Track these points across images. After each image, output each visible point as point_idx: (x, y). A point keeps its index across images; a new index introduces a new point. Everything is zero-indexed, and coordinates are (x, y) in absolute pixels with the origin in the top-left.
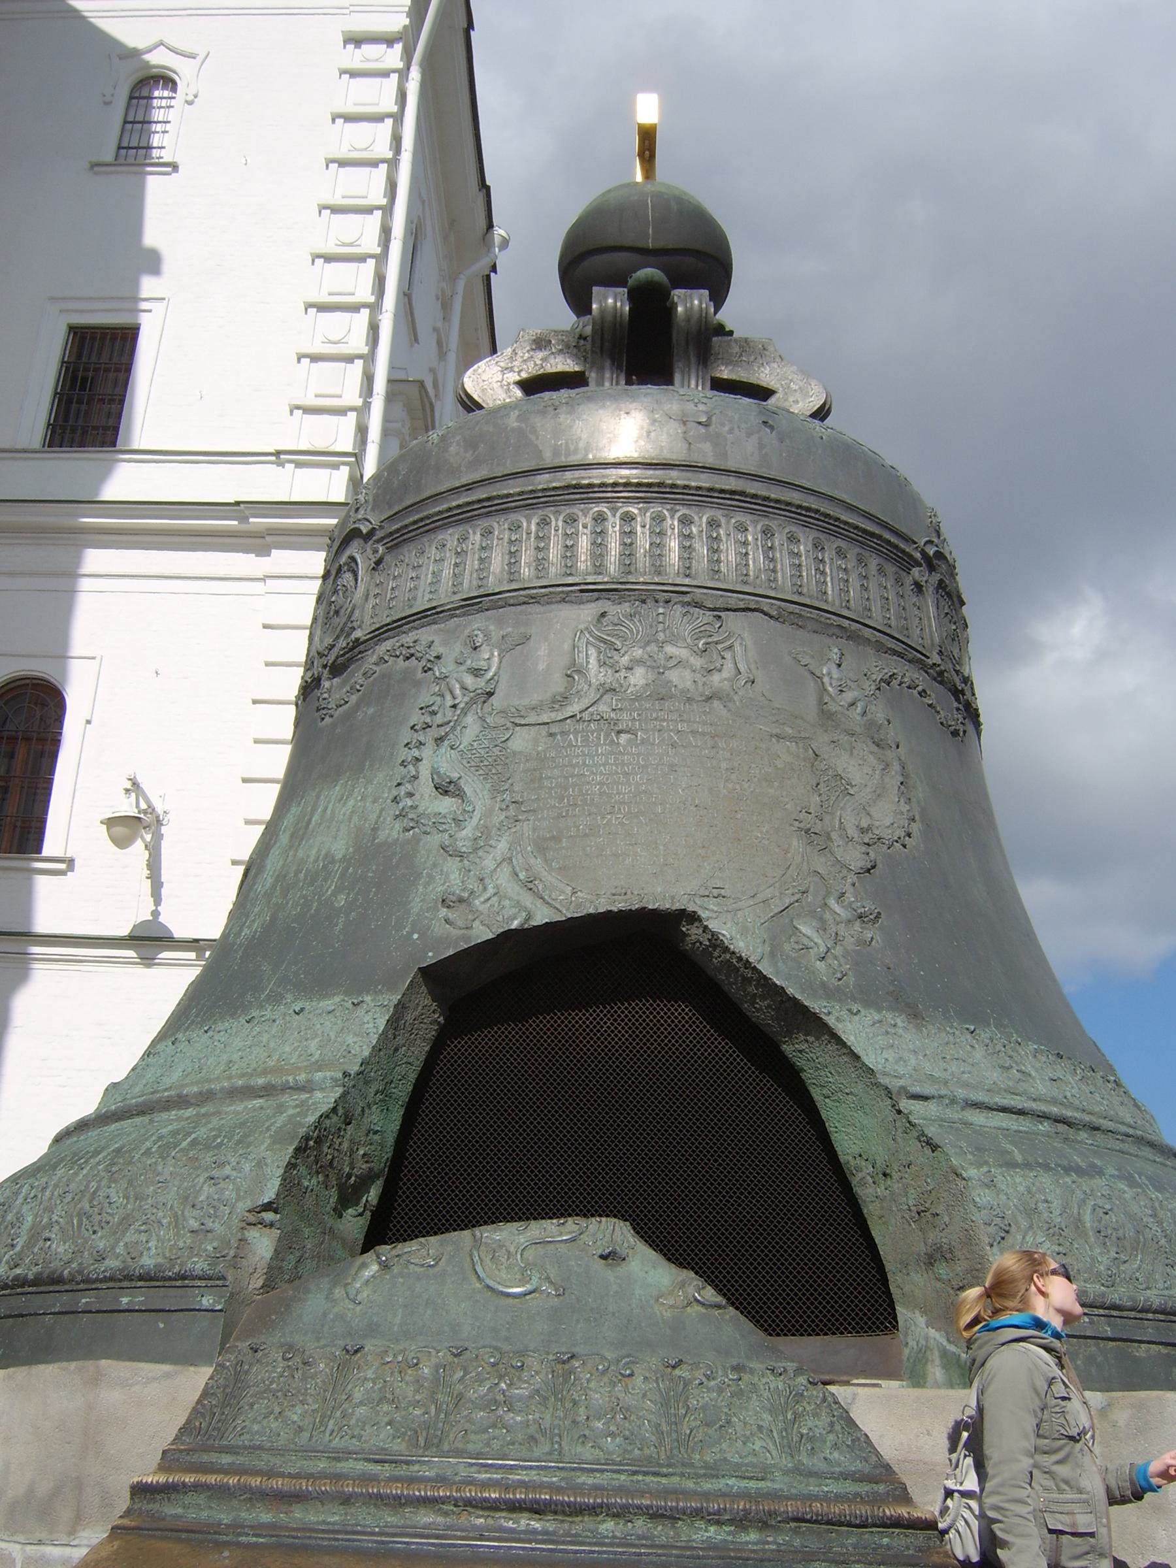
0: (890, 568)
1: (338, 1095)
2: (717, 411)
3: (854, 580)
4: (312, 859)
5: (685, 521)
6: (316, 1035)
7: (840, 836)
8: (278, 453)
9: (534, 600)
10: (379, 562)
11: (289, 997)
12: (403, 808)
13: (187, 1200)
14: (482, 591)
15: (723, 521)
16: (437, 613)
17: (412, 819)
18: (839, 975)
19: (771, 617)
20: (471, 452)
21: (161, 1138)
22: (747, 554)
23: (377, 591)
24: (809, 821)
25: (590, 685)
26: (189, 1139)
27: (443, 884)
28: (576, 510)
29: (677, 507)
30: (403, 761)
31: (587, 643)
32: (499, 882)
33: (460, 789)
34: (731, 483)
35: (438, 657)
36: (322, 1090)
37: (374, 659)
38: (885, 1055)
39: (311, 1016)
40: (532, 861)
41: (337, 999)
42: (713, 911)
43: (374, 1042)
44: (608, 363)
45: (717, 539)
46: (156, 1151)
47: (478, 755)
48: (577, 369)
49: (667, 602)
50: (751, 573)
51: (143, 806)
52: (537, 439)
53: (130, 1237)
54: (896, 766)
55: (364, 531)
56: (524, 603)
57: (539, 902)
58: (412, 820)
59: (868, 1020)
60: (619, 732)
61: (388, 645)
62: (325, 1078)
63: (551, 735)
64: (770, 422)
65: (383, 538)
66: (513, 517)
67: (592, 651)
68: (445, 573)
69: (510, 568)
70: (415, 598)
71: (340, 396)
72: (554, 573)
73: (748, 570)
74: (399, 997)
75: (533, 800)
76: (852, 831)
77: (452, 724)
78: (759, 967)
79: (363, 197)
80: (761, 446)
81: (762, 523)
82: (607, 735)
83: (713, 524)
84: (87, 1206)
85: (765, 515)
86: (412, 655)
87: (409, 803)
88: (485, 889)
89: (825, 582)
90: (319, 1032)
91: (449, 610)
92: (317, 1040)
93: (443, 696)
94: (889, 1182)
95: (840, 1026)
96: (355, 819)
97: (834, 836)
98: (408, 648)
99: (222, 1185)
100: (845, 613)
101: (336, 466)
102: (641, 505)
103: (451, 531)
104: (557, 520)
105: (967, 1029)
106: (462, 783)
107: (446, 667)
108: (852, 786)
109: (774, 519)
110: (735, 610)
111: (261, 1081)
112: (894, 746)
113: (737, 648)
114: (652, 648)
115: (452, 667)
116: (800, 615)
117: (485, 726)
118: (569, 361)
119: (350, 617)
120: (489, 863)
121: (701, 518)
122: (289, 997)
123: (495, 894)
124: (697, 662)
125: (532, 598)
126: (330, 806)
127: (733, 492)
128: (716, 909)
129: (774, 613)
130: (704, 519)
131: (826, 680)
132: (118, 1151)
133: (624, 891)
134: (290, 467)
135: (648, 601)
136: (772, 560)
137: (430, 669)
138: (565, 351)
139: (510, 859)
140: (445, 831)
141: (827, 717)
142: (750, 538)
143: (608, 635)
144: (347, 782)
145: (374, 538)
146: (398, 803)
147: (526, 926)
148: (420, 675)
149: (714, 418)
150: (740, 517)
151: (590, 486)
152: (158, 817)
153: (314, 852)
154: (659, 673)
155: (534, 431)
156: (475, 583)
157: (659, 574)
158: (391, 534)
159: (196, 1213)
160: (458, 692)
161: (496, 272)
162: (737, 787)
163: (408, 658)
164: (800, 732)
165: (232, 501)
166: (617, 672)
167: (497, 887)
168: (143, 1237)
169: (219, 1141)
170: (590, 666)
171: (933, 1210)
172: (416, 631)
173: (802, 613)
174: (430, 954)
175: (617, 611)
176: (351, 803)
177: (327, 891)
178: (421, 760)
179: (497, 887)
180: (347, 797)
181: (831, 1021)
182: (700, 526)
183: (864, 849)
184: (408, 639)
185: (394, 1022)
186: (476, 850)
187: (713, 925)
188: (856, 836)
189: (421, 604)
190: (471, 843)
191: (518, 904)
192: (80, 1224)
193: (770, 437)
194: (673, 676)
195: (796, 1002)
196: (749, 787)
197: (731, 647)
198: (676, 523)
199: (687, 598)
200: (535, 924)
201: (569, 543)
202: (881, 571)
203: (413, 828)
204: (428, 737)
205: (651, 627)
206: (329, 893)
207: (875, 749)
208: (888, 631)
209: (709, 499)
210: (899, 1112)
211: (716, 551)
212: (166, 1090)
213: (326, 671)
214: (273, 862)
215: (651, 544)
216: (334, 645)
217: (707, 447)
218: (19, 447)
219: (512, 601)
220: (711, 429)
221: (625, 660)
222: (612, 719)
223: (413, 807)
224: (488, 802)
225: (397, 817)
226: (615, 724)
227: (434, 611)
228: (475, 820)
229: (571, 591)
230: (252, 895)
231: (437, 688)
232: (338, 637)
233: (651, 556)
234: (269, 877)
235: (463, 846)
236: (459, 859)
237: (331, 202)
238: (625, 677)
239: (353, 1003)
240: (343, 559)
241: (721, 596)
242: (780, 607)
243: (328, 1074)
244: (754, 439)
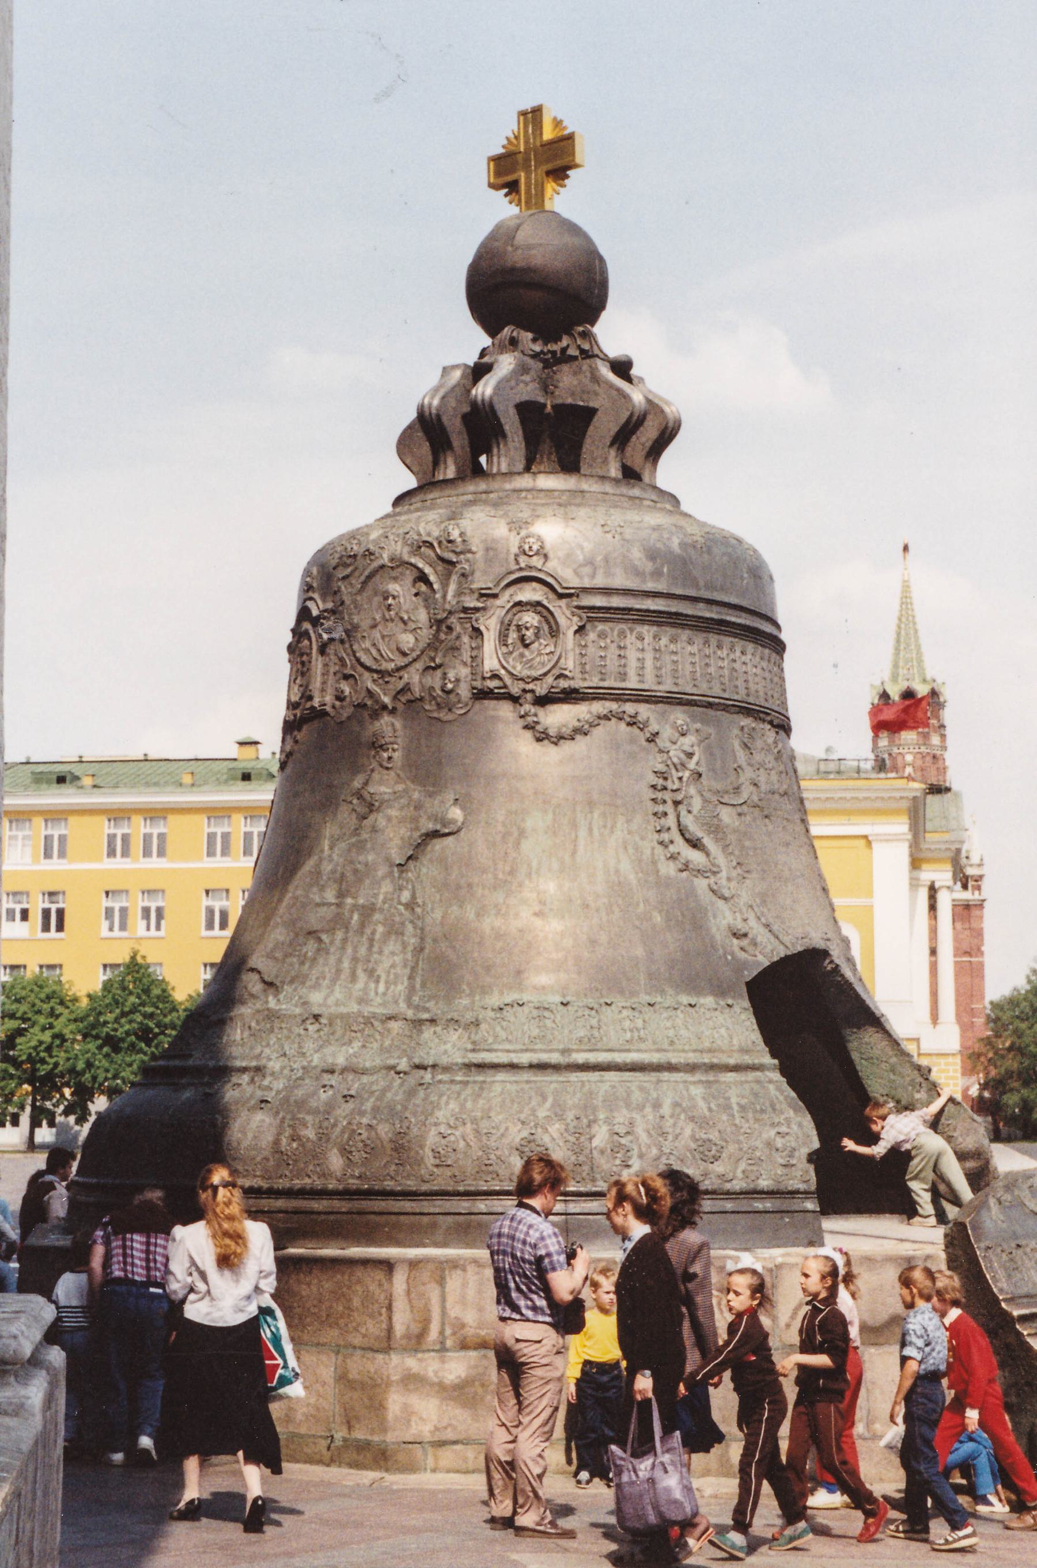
9: (710, 705)
13: (769, 1144)
33: (704, 845)
35: (657, 733)
53: (742, 1166)
56: (706, 707)
66: (688, 632)
68: (649, 664)
72: (717, 691)
84: (693, 1146)
86: (634, 723)
96: (631, 851)
99: (787, 1137)
103: (646, 627)
107: (662, 742)
115: (668, 744)
117: (706, 801)
132: (676, 1105)
137: (653, 741)
146: (666, 847)
160: (679, 767)
168: (755, 1168)
176: (618, 833)
184: (630, 708)
187: (837, 961)
189: (632, 683)
192: (694, 1157)
199: (769, 718)
204: (667, 796)
206: (642, 905)
223: (679, 853)
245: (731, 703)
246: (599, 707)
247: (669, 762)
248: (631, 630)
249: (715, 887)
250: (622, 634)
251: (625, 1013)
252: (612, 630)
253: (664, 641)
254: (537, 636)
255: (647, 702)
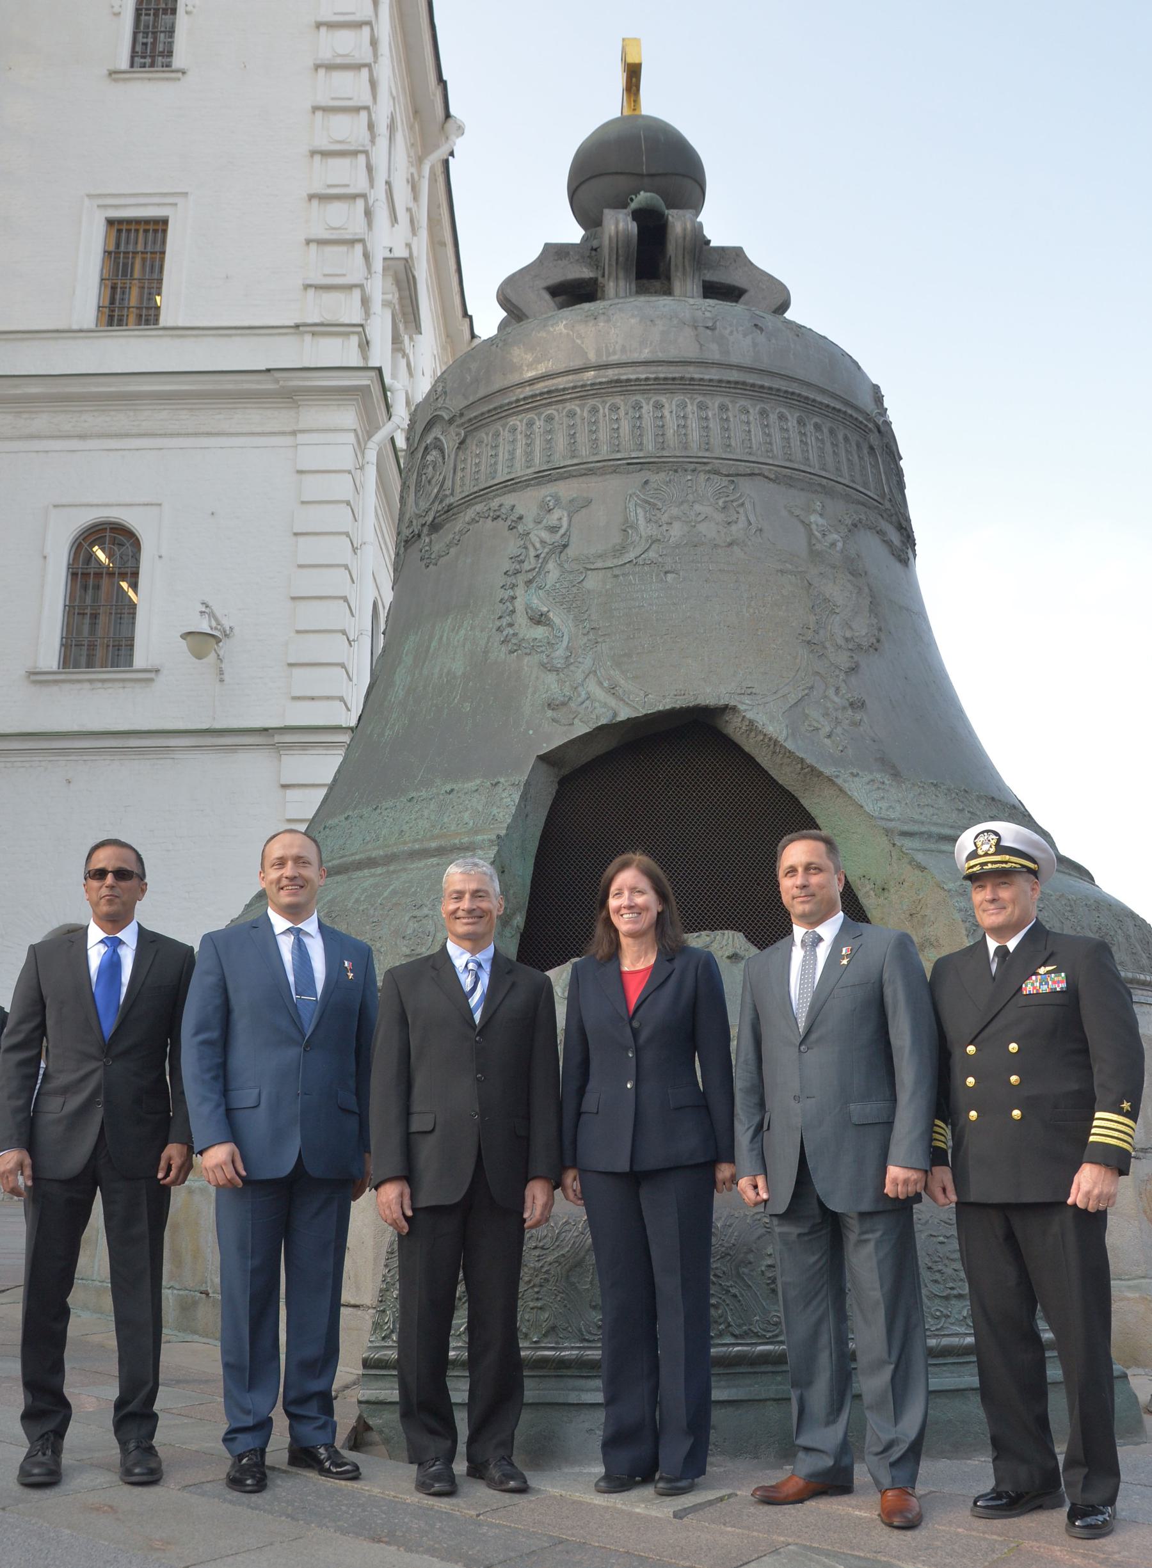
0: (854, 438)
1: (495, 852)
2: (719, 318)
3: (828, 448)
4: (436, 676)
5: (702, 407)
6: (467, 809)
7: (832, 645)
8: (297, 326)
10: (461, 443)
11: (438, 781)
12: (507, 636)
14: (550, 466)
15: (730, 406)
16: (516, 483)
17: (515, 644)
18: (840, 748)
19: (770, 479)
20: (530, 354)
21: (365, 890)
22: (749, 431)
23: (463, 466)
24: (809, 635)
25: (641, 537)
26: (389, 890)
27: (547, 691)
28: (618, 400)
29: (695, 396)
30: (502, 599)
31: (636, 504)
32: (589, 689)
33: (549, 619)
34: (734, 376)
35: (521, 518)
36: (481, 848)
37: (467, 519)
38: (879, 805)
39: (460, 795)
40: (612, 672)
41: (478, 782)
42: (748, 705)
43: (514, 812)
44: (621, 275)
45: (727, 420)
46: (364, 901)
47: (560, 593)
48: (592, 275)
49: (694, 471)
50: (754, 446)
51: (214, 624)
52: (583, 343)
54: (866, 590)
55: (447, 418)
57: (621, 704)
58: (514, 644)
59: (866, 779)
60: (666, 573)
61: (479, 507)
62: (484, 840)
63: (616, 576)
64: (760, 324)
65: (463, 424)
66: (569, 406)
67: (639, 510)
68: (518, 452)
69: (571, 447)
70: (495, 472)
71: (344, 275)
72: (604, 452)
73: (751, 443)
74: (526, 778)
75: (607, 627)
76: (840, 641)
77: (537, 570)
78: (785, 744)
79: (350, 99)
80: (755, 345)
81: (758, 408)
82: (657, 575)
83: (723, 408)
85: (761, 399)
86: (499, 516)
87: (511, 632)
88: (579, 695)
89: (807, 451)
90: (469, 806)
91: (526, 481)
92: (469, 812)
93: (526, 548)
94: (886, 894)
95: (846, 785)
97: (827, 644)
98: (495, 511)
99: (424, 921)
100: (823, 473)
101: (347, 335)
102: (668, 395)
103: (520, 417)
104: (604, 409)
105: (932, 783)
106: (551, 615)
108: (837, 607)
109: (768, 402)
110: (744, 475)
111: (434, 845)
112: (863, 575)
113: (748, 506)
114: (685, 506)
115: (531, 525)
116: (791, 478)
117: (563, 571)
118: (585, 270)
119: (442, 486)
120: (579, 676)
121: (713, 404)
122: (438, 781)
123: (588, 699)
124: (720, 517)
125: (590, 470)
126: (445, 635)
127: (737, 383)
128: (750, 703)
129: (773, 476)
130: (716, 405)
131: (814, 527)
133: (683, 693)
134: (308, 338)
135: (679, 470)
136: (769, 435)
137: (515, 527)
138: (581, 261)
139: (595, 672)
140: (542, 652)
141: (815, 555)
142: (751, 418)
143: (651, 498)
144: (456, 616)
145: (455, 424)
147: (614, 721)
148: (507, 533)
149: (718, 323)
150: (742, 402)
151: (628, 380)
152: (225, 632)
153: (437, 670)
154: (692, 526)
155: (580, 337)
156: (546, 459)
157: (686, 448)
158: (470, 420)
159: (405, 942)
160: (538, 545)
161: (453, 157)
162: (756, 611)
163: (495, 519)
164: (797, 567)
165: (264, 368)
166: (660, 526)
167: (588, 693)
169: (413, 890)
170: (639, 522)
171: (922, 913)
172: (499, 498)
173: (793, 476)
174: (545, 745)
175: (657, 478)
176: (462, 632)
177: (454, 700)
178: (516, 598)
179: (588, 693)
180: (459, 628)
181: (839, 781)
182: (713, 410)
183: (849, 654)
184: (494, 504)
185: (524, 797)
186: (568, 666)
187: (749, 715)
188: (843, 644)
190: (563, 661)
191: (605, 705)
193: (761, 338)
194: (702, 528)
195: (813, 769)
196: (765, 611)
197: (742, 504)
198: (695, 409)
199: (708, 468)
200: (621, 720)
201: (616, 426)
202: (846, 439)
203: (516, 650)
204: (521, 579)
205: (683, 490)
206: (456, 701)
207: (851, 578)
208: (854, 486)
209: (718, 389)
210: (894, 845)
211: (727, 429)
212: (352, 854)
213: (425, 530)
214: (401, 678)
215: (678, 426)
216: (430, 509)
217: (714, 347)
218: (75, 327)
219: (574, 474)
220: (717, 332)
221: (665, 518)
222: (660, 563)
223: (515, 635)
224: (573, 629)
225: (503, 642)
226: (662, 566)
227: (512, 482)
228: (565, 643)
229: (620, 465)
230: (386, 703)
231: (522, 542)
232: (433, 502)
233: (679, 435)
234: (400, 691)
235: (559, 663)
236: (555, 673)
237: (323, 104)
238: (667, 530)
239: (492, 784)
240: (429, 439)
241: (733, 465)
242: (776, 471)
243: (485, 837)
244: (749, 339)
245: (625, 462)
246: (470, 513)
247: (528, 543)
248: (504, 426)
249: (545, 661)
250: (497, 435)
251: (385, 813)
252: (487, 434)
253: (539, 423)
254: (434, 467)
255: (514, 491)
